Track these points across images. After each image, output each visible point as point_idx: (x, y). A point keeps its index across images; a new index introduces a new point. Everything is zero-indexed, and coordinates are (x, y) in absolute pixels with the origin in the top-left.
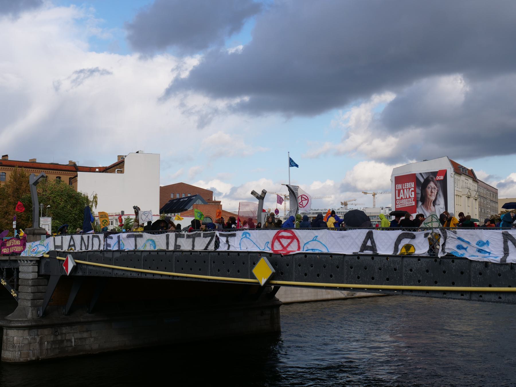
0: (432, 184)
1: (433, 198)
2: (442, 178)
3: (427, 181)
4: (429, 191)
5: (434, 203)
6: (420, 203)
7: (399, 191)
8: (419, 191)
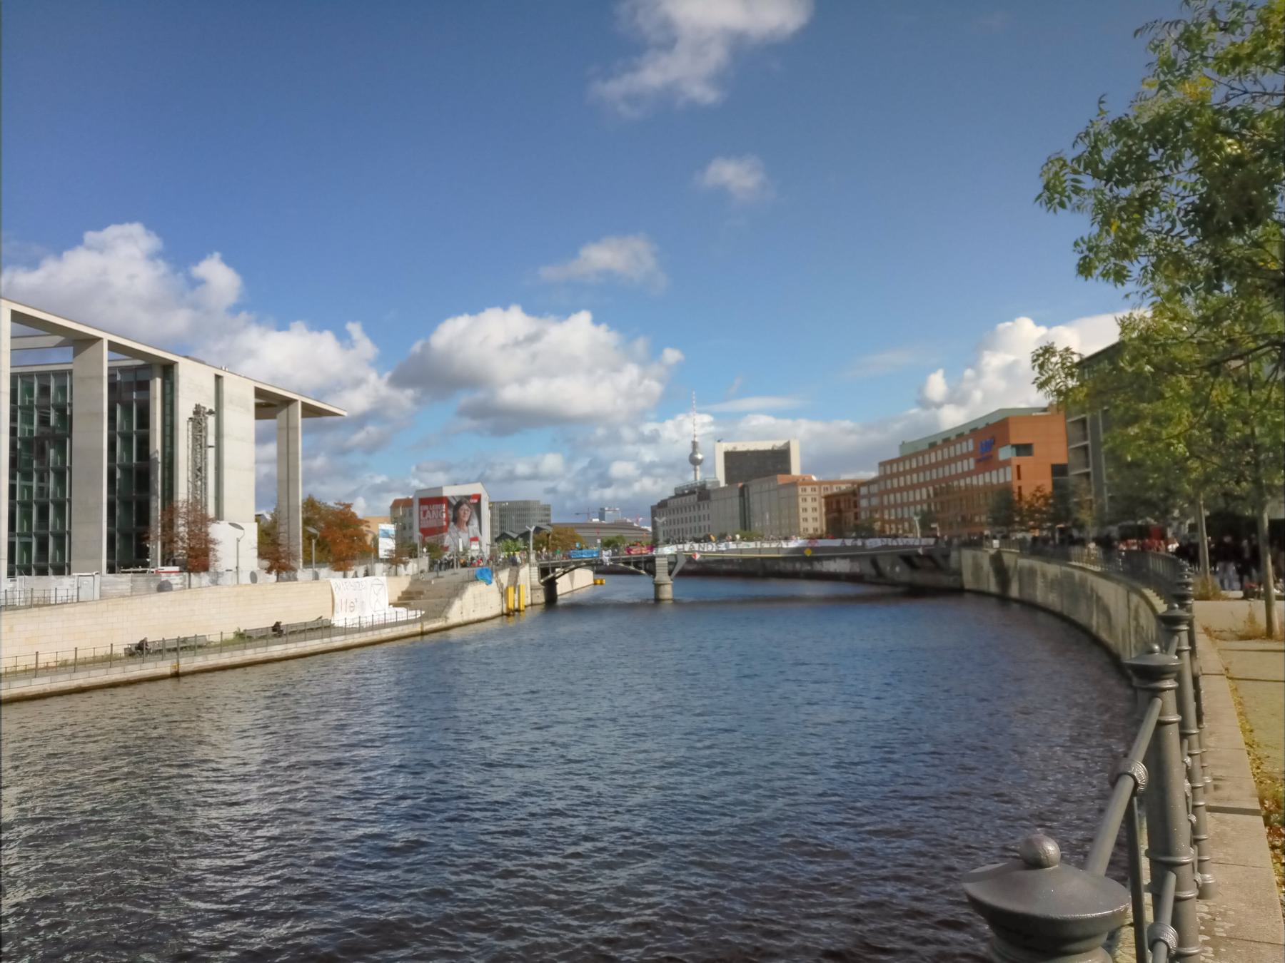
0: (465, 507)
1: (466, 519)
2: (476, 501)
3: (459, 504)
4: (462, 513)
5: (468, 523)
6: (452, 524)
7: (425, 513)
8: (451, 512)
